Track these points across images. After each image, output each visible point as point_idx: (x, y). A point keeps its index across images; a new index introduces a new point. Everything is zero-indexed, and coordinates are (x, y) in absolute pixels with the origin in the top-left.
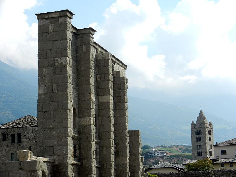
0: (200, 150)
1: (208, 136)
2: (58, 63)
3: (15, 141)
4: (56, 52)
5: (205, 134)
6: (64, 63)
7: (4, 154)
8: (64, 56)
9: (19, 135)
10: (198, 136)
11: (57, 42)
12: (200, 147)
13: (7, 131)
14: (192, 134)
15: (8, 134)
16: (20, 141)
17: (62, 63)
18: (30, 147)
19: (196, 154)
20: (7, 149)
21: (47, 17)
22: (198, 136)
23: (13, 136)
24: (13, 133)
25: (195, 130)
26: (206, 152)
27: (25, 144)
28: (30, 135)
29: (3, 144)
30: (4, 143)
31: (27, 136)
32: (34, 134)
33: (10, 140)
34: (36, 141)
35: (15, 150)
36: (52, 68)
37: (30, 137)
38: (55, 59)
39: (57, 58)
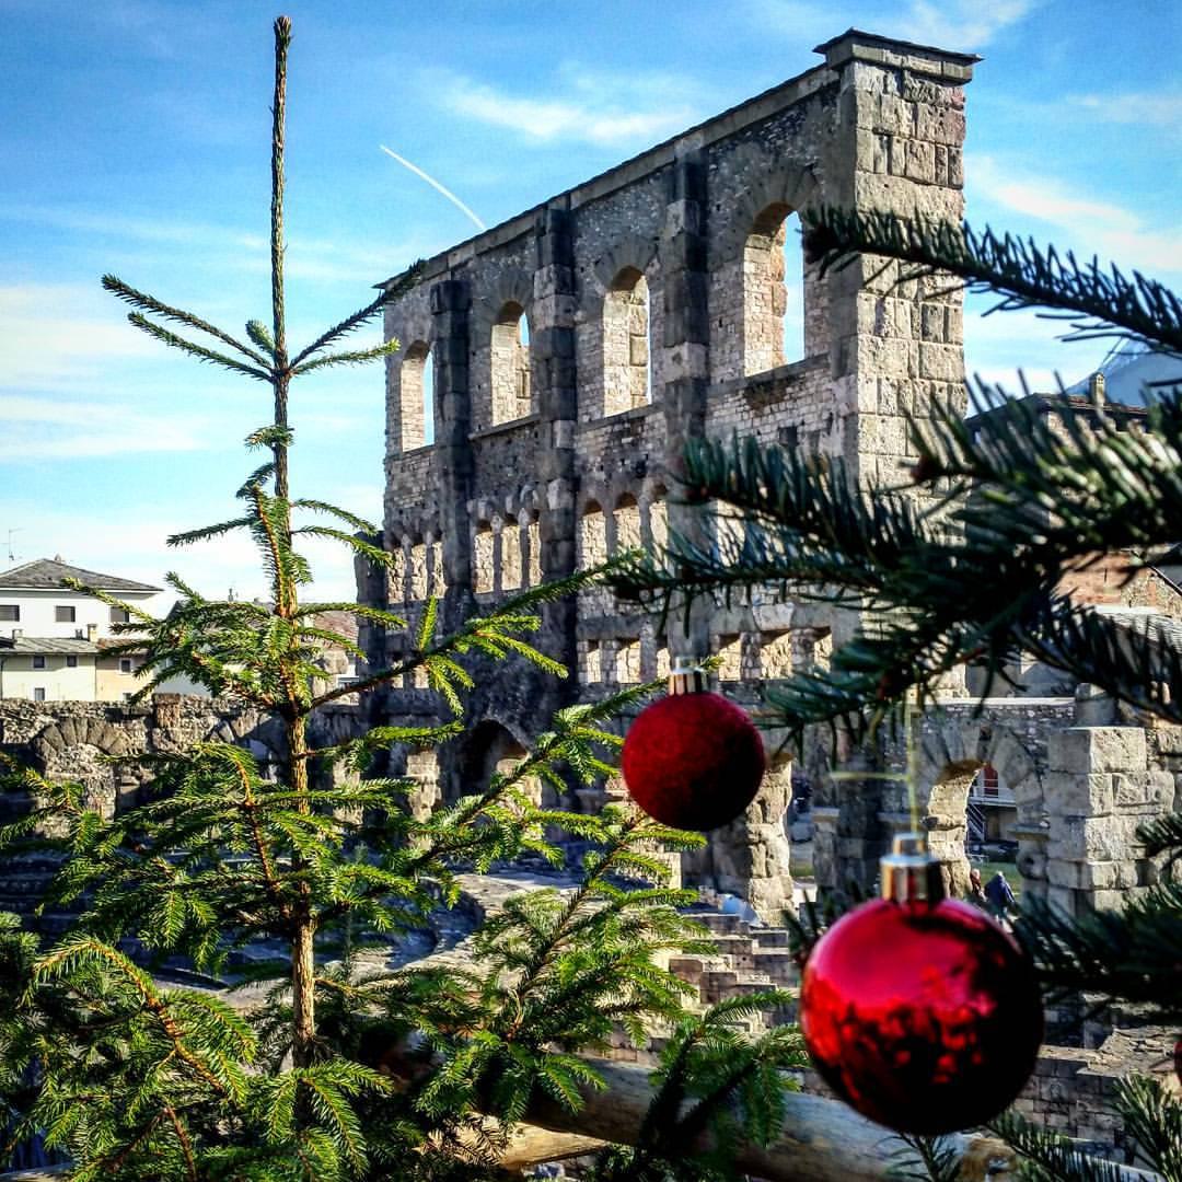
21: (895, 60)
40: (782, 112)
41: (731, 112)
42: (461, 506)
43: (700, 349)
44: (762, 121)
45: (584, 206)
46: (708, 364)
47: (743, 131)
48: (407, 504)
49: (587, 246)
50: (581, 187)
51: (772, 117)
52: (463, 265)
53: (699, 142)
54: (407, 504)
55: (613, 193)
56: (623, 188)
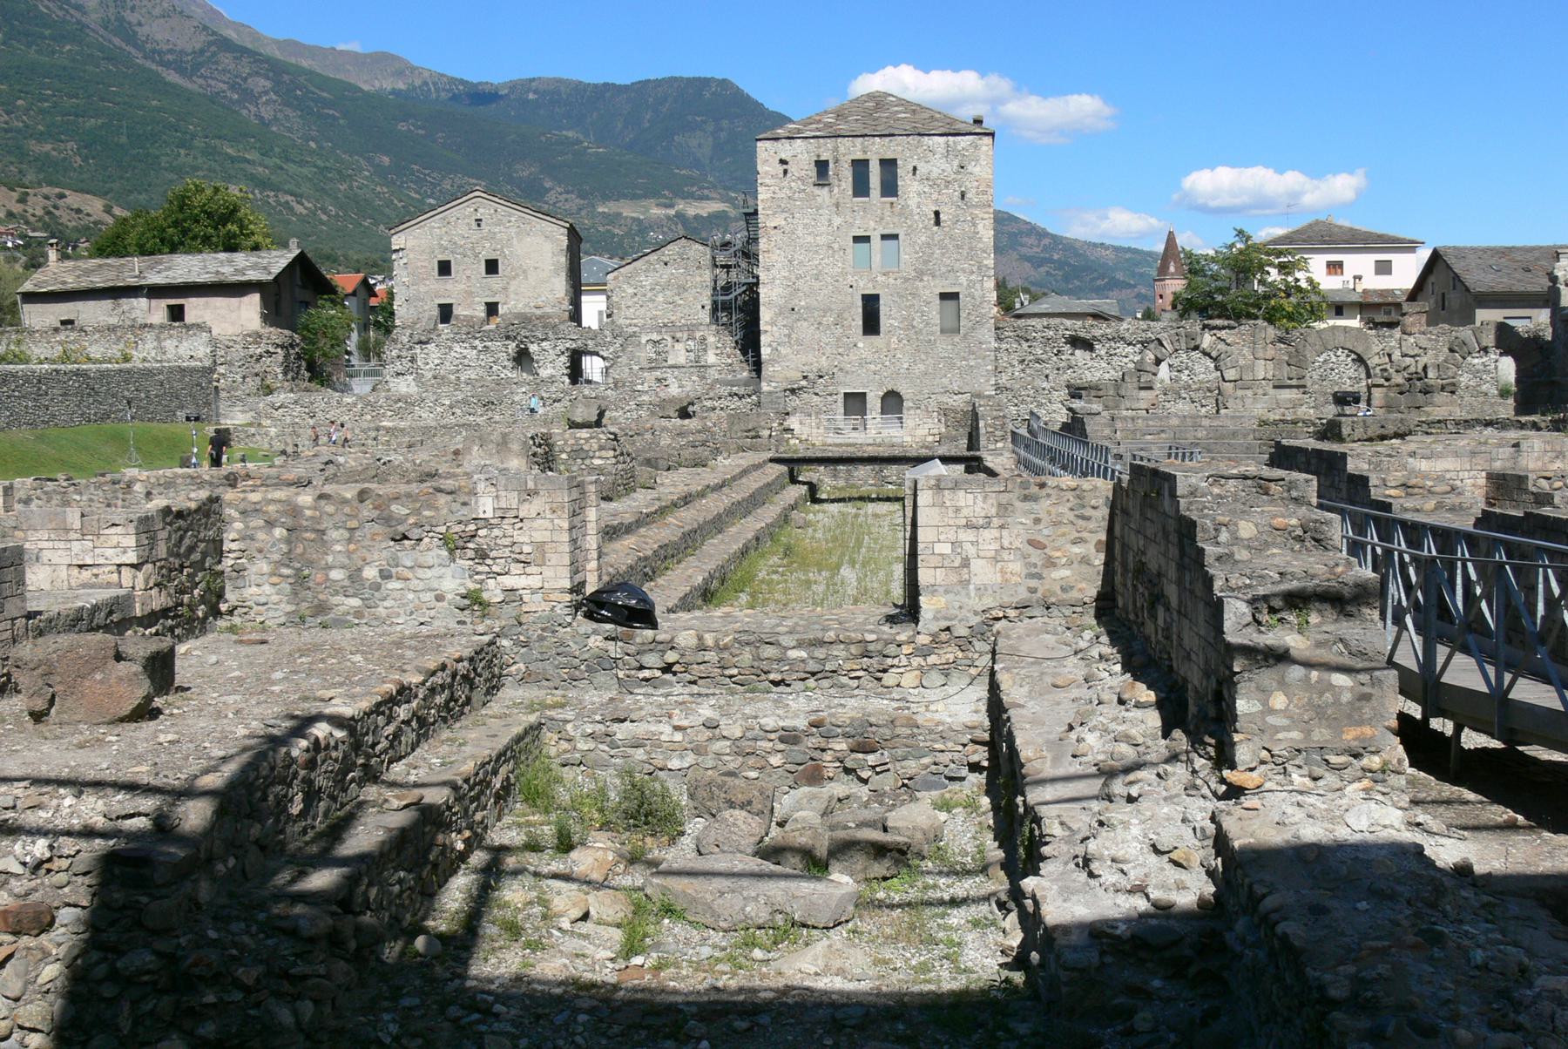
3: (868, 189)
7: (822, 240)
9: (889, 165)
13: (836, 149)
15: (837, 161)
16: (890, 188)
18: (937, 214)
20: (837, 221)
23: (860, 167)
24: (859, 156)
27: (913, 203)
29: (815, 197)
32: (956, 163)
33: (847, 183)
34: (963, 196)
35: (872, 224)
37: (934, 175)
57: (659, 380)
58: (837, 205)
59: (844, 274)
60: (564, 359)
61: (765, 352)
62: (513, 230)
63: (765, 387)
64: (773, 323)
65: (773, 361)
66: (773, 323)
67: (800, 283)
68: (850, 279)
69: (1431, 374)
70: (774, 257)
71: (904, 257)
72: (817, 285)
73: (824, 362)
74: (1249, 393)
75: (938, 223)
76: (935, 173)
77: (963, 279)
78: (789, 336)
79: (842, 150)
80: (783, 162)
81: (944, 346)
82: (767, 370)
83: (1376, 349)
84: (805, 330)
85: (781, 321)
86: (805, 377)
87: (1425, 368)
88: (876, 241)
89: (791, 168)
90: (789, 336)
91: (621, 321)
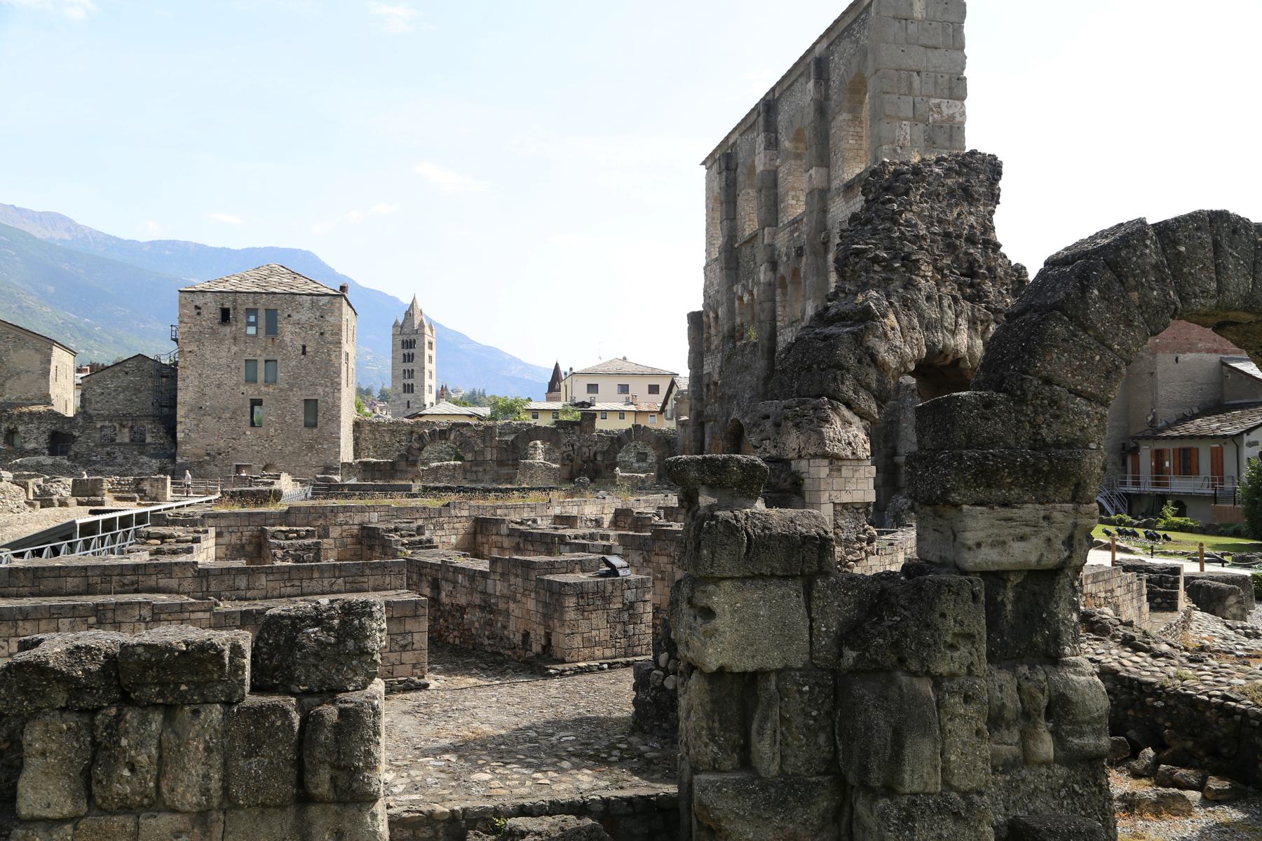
0: (410, 381)
1: (427, 352)
2: (940, 113)
4: (936, 83)
5: (423, 348)
6: (958, 119)
7: (223, 361)
8: (958, 99)
10: (406, 351)
11: (937, 52)
12: (410, 374)
13: (235, 301)
14: (394, 345)
17: (952, 117)
18: (304, 347)
19: (401, 389)
20: (234, 349)
22: (406, 351)
24: (251, 306)
25: (401, 338)
26: (423, 386)
27: (287, 339)
28: (304, 315)
30: (227, 330)
31: (295, 317)
32: (318, 314)
34: (322, 334)
36: (921, 126)
37: (303, 321)
38: (934, 101)
39: (938, 101)
40: (858, 17)
41: (836, 22)
42: (730, 289)
43: (823, 171)
44: (851, 24)
45: (781, 95)
46: (829, 180)
47: (843, 32)
48: (712, 293)
49: (782, 119)
50: (779, 83)
51: (855, 21)
52: (735, 143)
53: (825, 44)
54: (712, 293)
55: (791, 85)
56: (796, 80)
57: (108, 454)
58: (235, 339)
59: (238, 385)
60: (45, 436)
61: (180, 436)
62: (10, 345)
63: (179, 460)
64: (186, 416)
65: (185, 443)
66: (186, 416)
67: (207, 390)
68: (242, 388)
69: (599, 458)
70: (189, 372)
71: (280, 375)
72: (218, 391)
73: (222, 444)
74: (481, 469)
75: (304, 353)
76: (304, 319)
77: (320, 390)
78: (197, 425)
79: (239, 301)
80: (197, 307)
81: (308, 434)
82: (182, 448)
83: (565, 441)
84: (209, 422)
85: (192, 415)
86: (208, 454)
87: (595, 454)
88: (261, 366)
89: (204, 312)
90: (197, 425)
91: (91, 412)
